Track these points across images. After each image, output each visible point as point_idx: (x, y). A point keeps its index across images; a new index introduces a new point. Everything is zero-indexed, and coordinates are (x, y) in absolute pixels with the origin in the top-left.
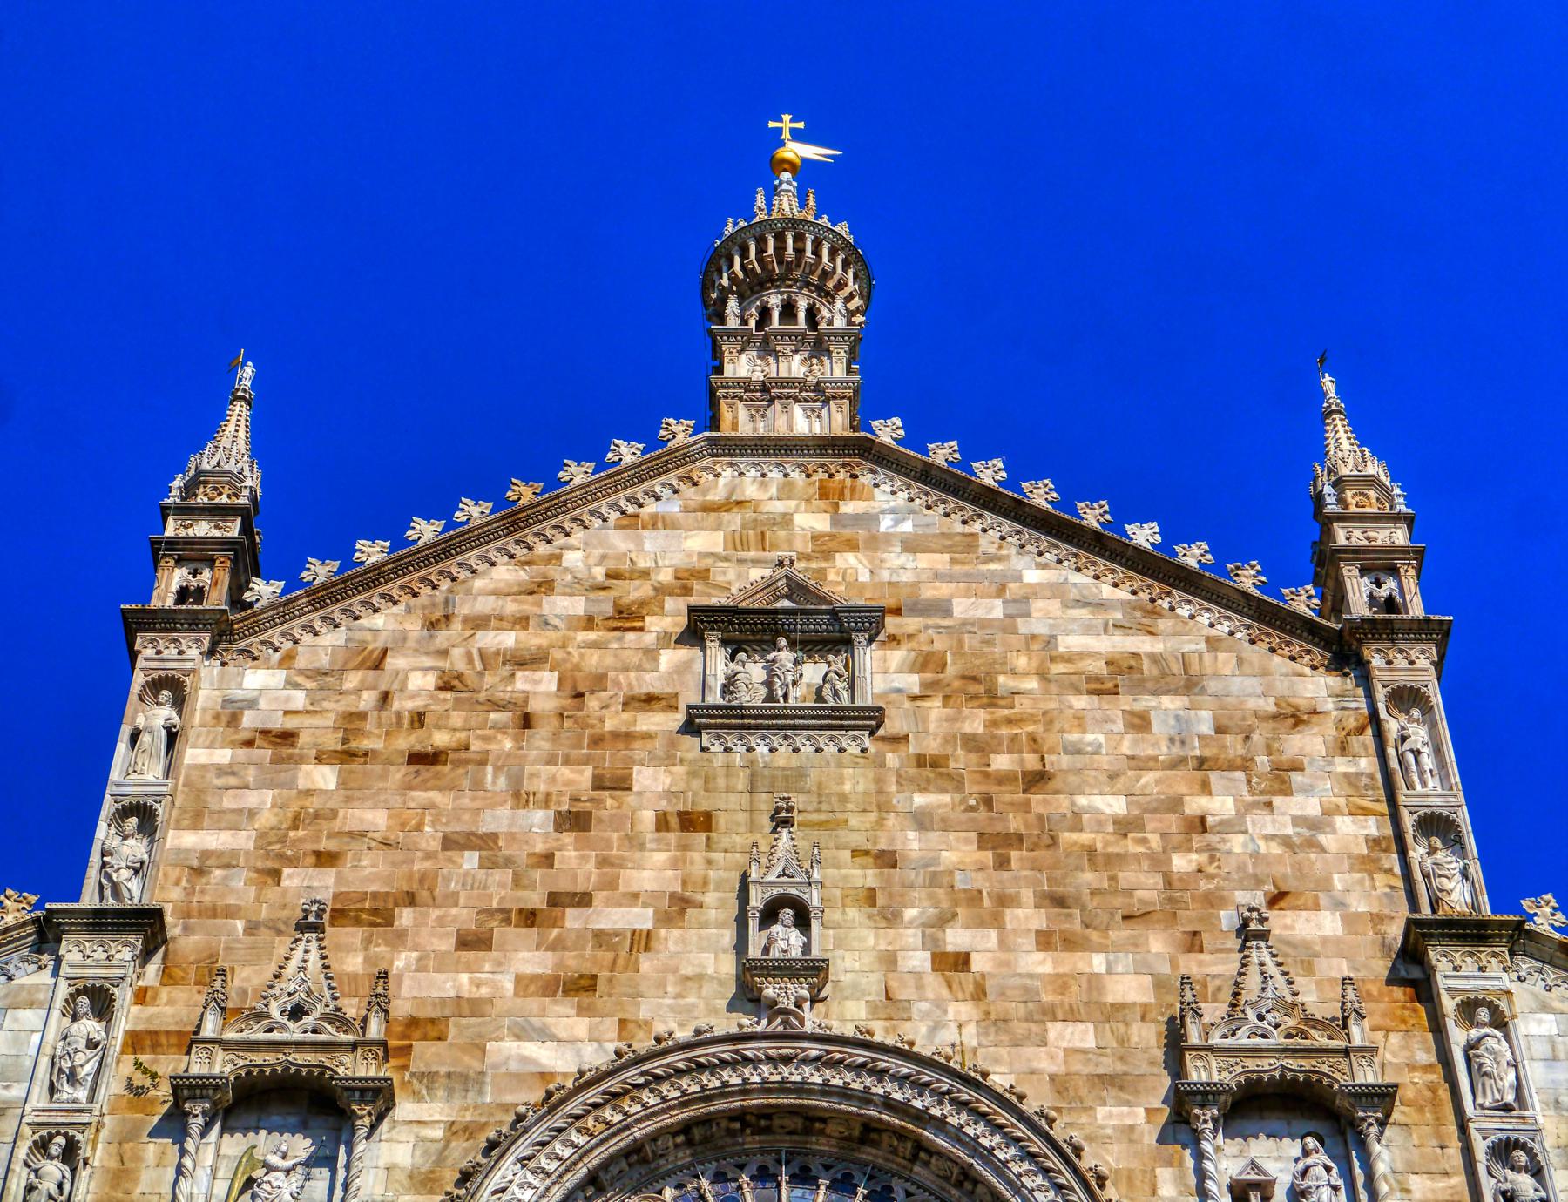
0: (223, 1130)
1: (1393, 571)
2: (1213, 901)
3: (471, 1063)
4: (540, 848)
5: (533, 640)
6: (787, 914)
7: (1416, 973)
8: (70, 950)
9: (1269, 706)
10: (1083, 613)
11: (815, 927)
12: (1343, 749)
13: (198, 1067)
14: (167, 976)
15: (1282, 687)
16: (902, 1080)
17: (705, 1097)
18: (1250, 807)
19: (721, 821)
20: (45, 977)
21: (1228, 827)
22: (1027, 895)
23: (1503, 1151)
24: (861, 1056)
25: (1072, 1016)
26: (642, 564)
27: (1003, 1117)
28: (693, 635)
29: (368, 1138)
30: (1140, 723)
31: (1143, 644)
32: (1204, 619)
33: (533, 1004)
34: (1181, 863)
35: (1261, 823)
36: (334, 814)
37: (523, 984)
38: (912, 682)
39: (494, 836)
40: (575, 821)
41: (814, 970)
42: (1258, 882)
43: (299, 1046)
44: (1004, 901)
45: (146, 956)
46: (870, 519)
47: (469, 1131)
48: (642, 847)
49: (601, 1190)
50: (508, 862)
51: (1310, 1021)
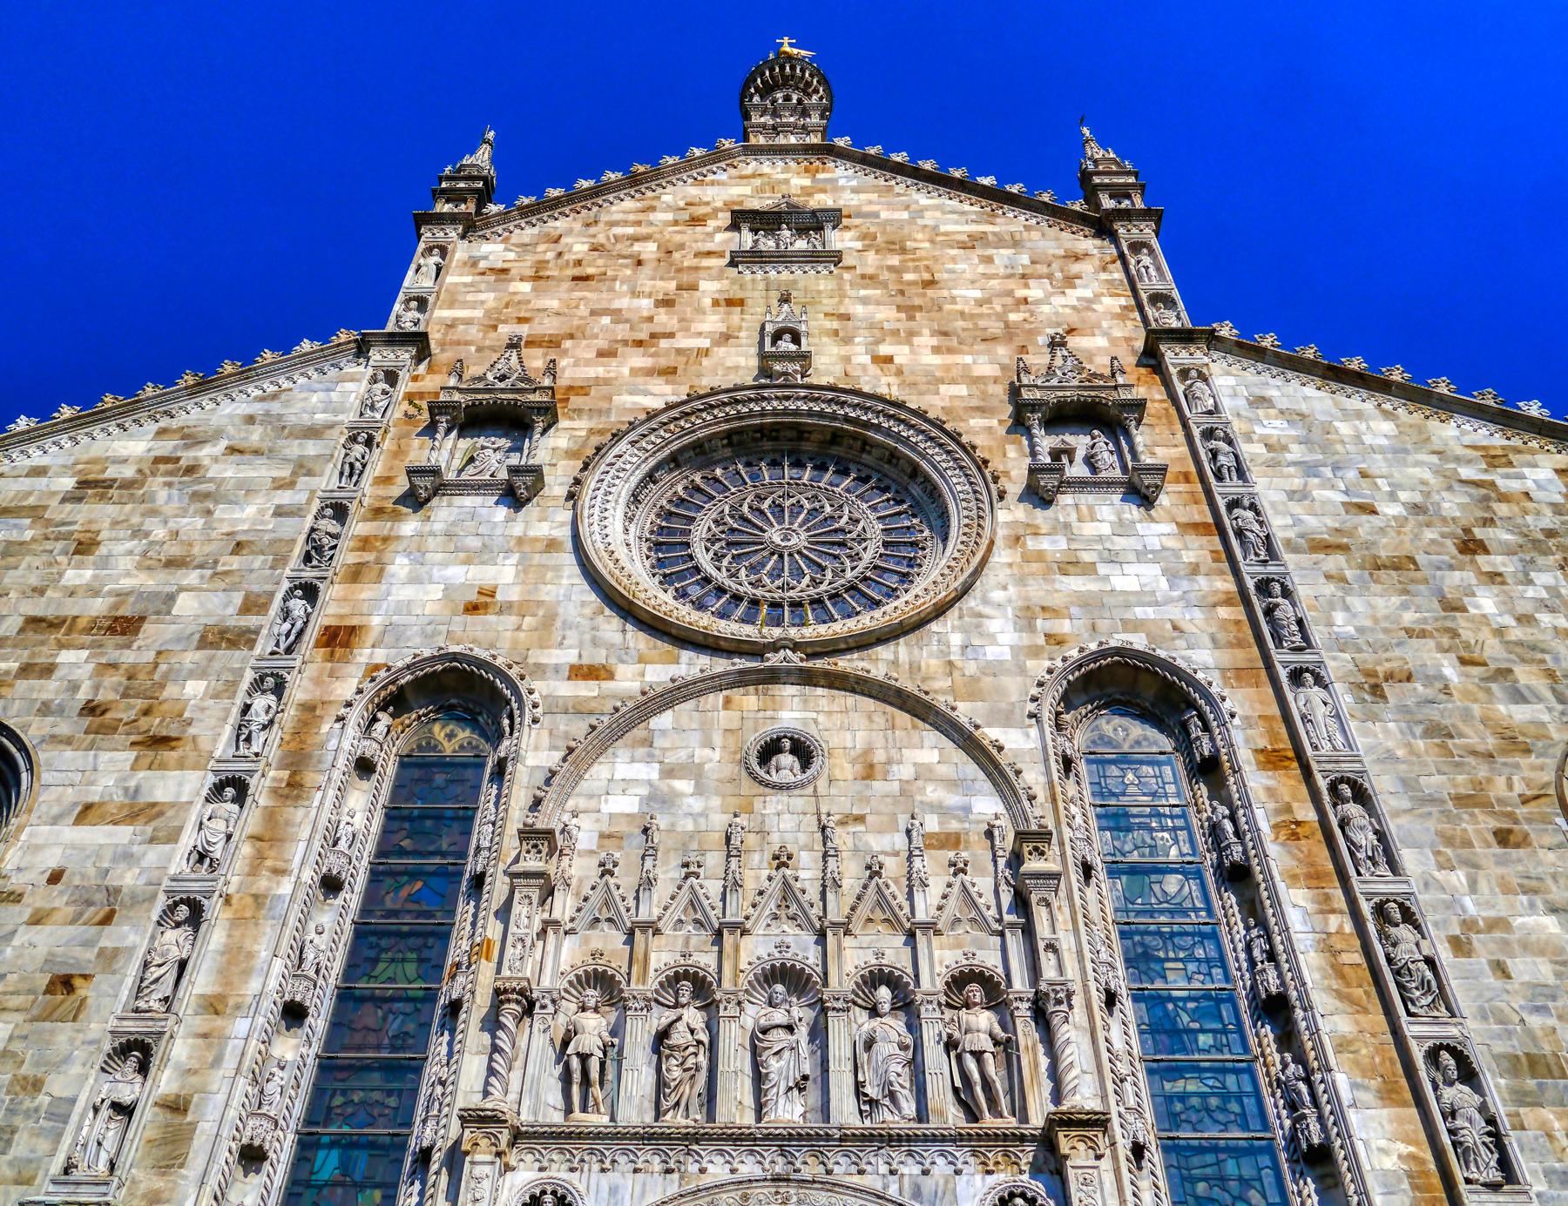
0: (460, 436)
1: (1128, 197)
2: (1032, 333)
3: (605, 405)
4: (645, 314)
5: (643, 230)
6: (787, 337)
7: (1152, 362)
8: (375, 355)
9: (1062, 252)
10: (955, 216)
11: (803, 341)
12: (1104, 269)
13: (443, 397)
14: (430, 370)
15: (1068, 245)
16: (855, 406)
17: (740, 417)
18: (1052, 294)
19: (750, 302)
20: (361, 369)
21: (1038, 302)
22: (926, 331)
23: (1209, 434)
24: (830, 395)
25: (953, 382)
26: (705, 199)
27: (914, 421)
28: (734, 226)
29: (542, 434)
30: (989, 260)
31: (988, 228)
32: (1022, 218)
33: (640, 380)
34: (1013, 317)
35: (1058, 300)
36: (529, 302)
37: (634, 372)
38: (859, 245)
39: (620, 310)
40: (667, 303)
41: (805, 357)
42: (1059, 325)
43: (503, 391)
44: (912, 334)
45: (419, 359)
46: (834, 181)
47: (601, 432)
48: (704, 313)
49: (678, 466)
50: (627, 321)
51: (1095, 375)
